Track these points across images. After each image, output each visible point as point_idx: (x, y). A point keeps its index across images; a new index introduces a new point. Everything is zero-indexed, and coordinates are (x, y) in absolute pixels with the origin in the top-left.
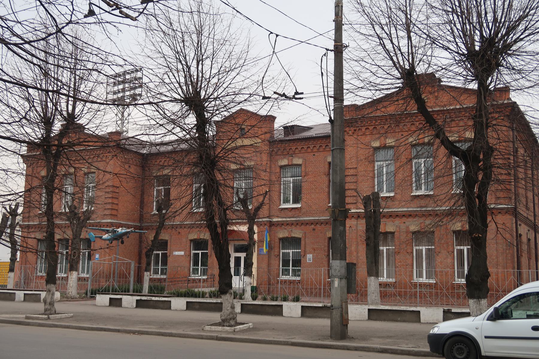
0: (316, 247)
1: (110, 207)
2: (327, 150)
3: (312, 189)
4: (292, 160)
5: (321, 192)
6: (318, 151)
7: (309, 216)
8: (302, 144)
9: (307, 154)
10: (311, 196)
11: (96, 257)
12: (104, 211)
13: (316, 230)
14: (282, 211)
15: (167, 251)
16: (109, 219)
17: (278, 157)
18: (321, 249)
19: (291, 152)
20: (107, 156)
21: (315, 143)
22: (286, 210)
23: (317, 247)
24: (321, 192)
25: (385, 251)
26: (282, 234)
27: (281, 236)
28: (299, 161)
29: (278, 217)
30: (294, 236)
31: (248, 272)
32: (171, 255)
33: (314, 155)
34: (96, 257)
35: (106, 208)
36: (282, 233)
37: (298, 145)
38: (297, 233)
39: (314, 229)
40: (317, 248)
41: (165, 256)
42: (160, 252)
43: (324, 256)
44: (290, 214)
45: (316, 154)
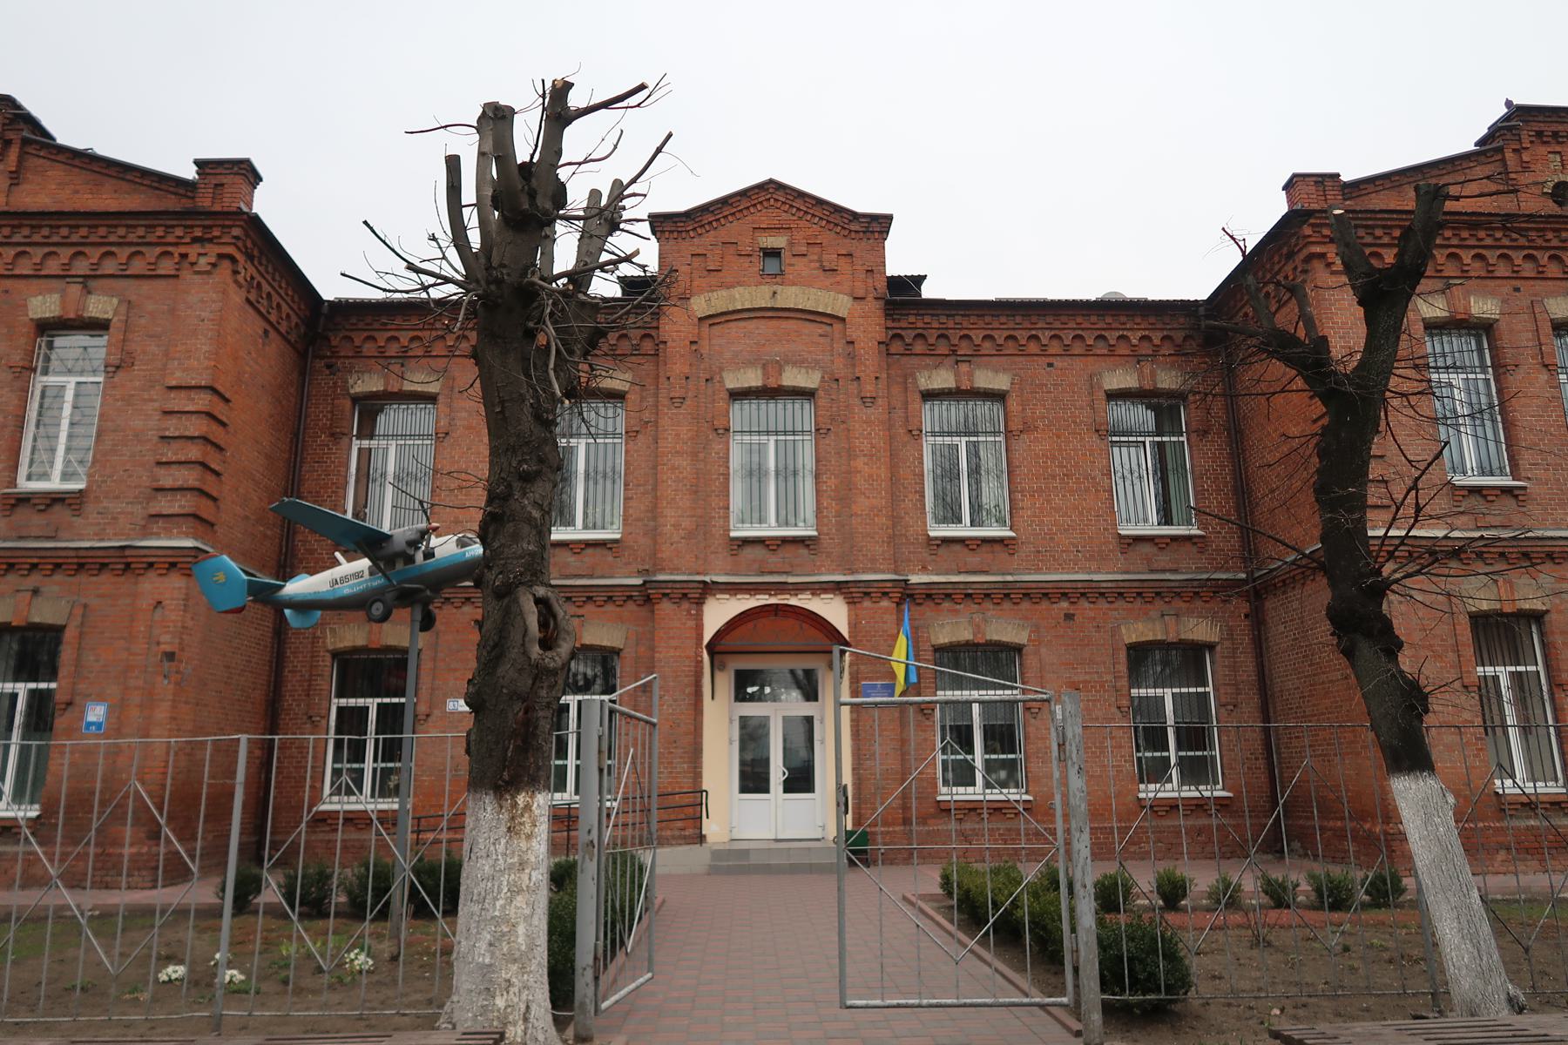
0: (1081, 678)
1: (192, 483)
2: (1099, 352)
3: (1054, 477)
4: (970, 375)
5: (1087, 490)
6: (1067, 352)
7: (1056, 571)
8: (1011, 325)
9: (1021, 359)
10: (1048, 501)
11: (91, 718)
12: (149, 499)
13: (1078, 619)
14: (941, 551)
15: (403, 695)
16: (187, 535)
17: (915, 361)
18: (1102, 686)
19: (965, 348)
20: (184, 256)
21: (1057, 325)
22: (957, 547)
23: (1087, 677)
24: (1087, 490)
25: (1504, 682)
26: (952, 628)
27: (943, 638)
28: (1000, 382)
29: (924, 569)
30: (995, 638)
31: (801, 780)
32: (436, 712)
33: (1050, 365)
34: (91, 718)
35: (167, 482)
36: (948, 628)
37: (995, 325)
38: (1004, 628)
39: (1069, 617)
40: (1085, 682)
41: (391, 718)
42: (372, 703)
43: (1114, 710)
44: (973, 560)
45: (1057, 362)
